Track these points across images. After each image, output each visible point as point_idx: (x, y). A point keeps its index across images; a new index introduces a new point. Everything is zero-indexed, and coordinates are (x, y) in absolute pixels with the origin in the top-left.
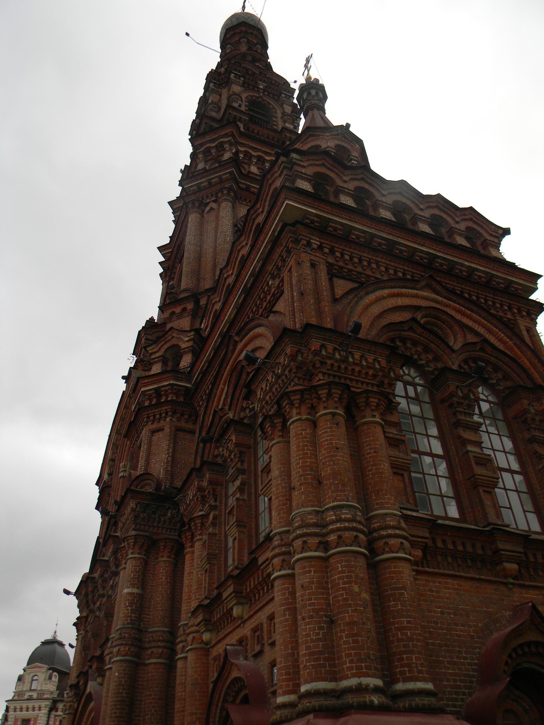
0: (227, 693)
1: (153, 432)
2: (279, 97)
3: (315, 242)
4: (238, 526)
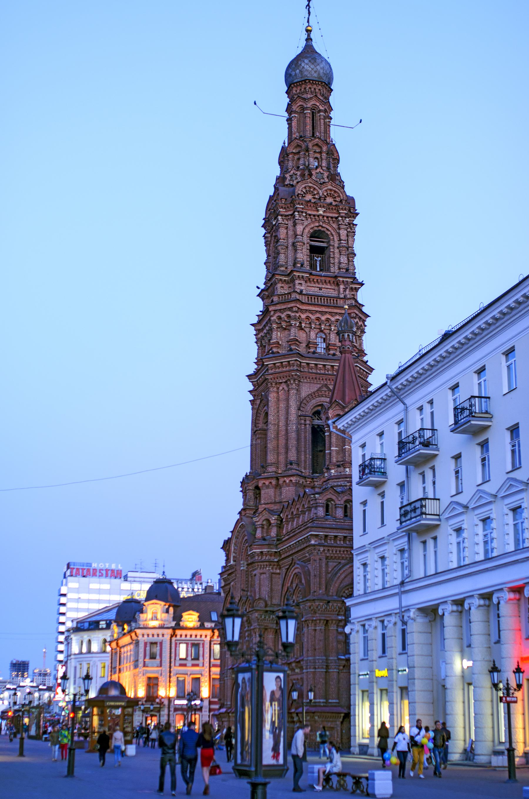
1: (261, 574)
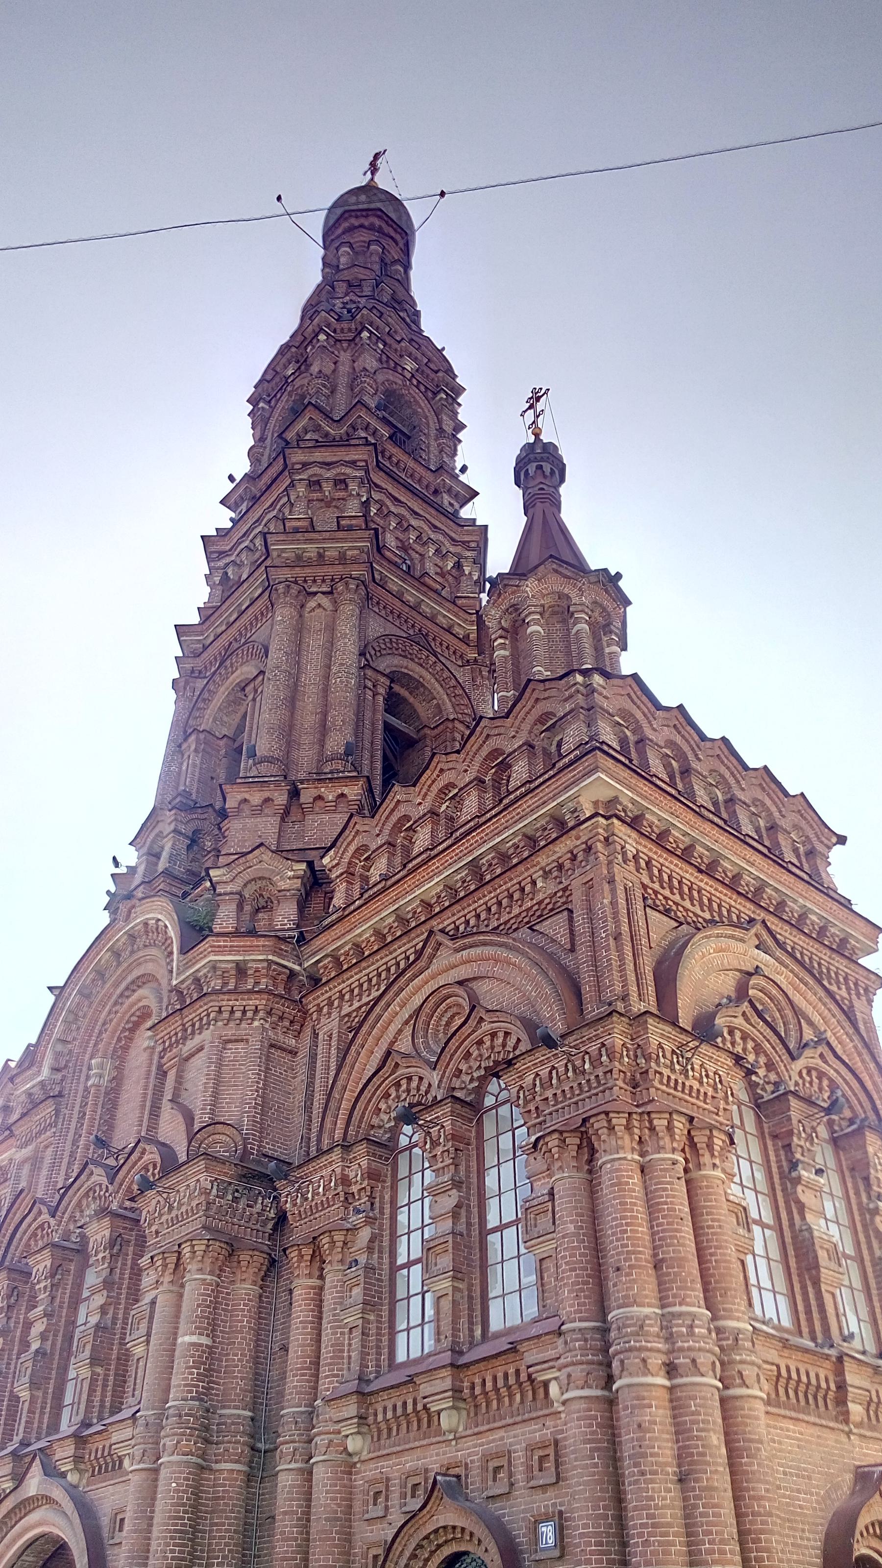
0: (419, 1546)
2: (435, 394)
3: (631, 850)
4: (454, 1278)
